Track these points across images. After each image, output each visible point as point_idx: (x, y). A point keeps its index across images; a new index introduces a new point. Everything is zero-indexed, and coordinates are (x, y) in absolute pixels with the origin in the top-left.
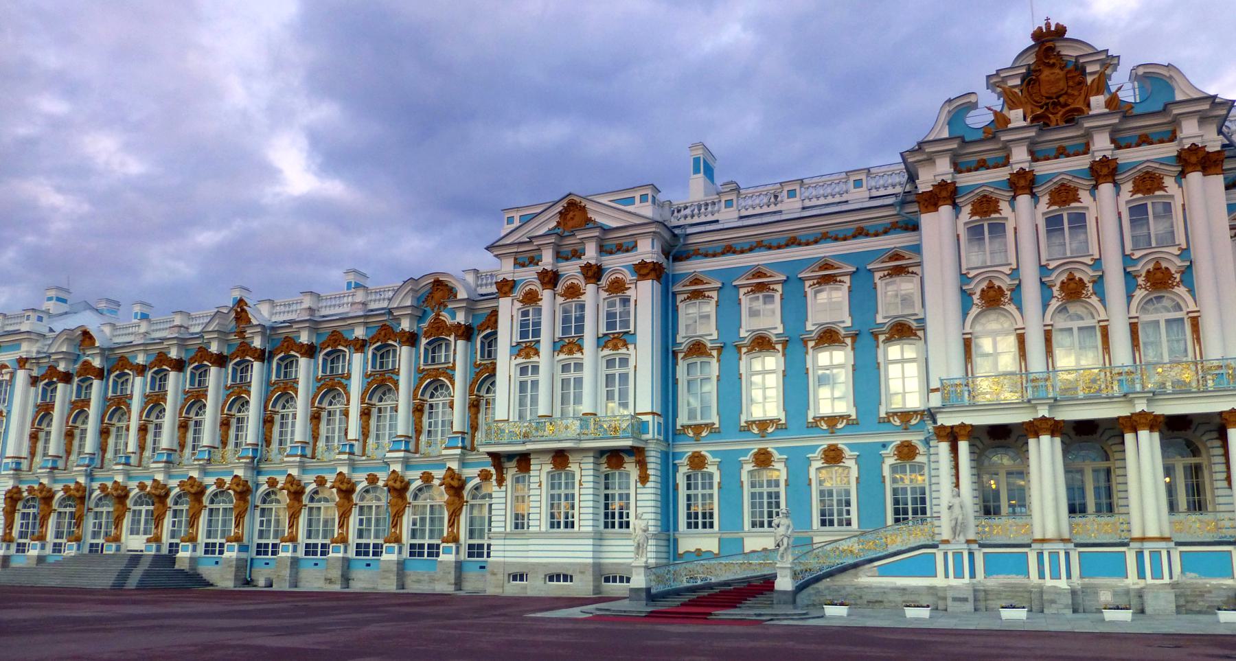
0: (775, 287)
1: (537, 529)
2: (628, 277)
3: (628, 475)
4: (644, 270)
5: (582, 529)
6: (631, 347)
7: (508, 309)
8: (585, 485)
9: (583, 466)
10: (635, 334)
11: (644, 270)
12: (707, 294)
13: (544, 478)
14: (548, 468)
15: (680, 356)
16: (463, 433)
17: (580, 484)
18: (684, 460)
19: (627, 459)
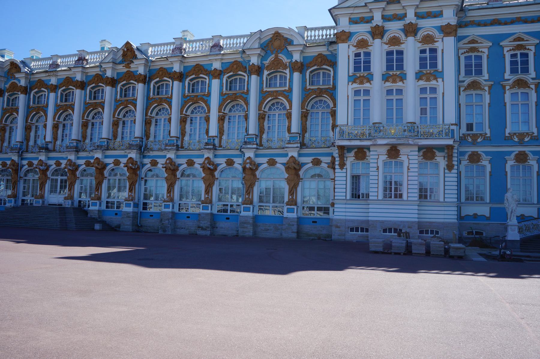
0: (530, 47)
1: (376, 198)
2: (437, 34)
3: (437, 165)
4: (447, 30)
5: (410, 199)
6: (440, 80)
7: (345, 53)
8: (412, 170)
9: (410, 157)
10: (442, 71)
11: (447, 30)
12: (480, 50)
13: (381, 165)
14: (384, 157)
15: (462, 89)
16: (300, 134)
17: (408, 169)
18: (466, 157)
19: (438, 153)
